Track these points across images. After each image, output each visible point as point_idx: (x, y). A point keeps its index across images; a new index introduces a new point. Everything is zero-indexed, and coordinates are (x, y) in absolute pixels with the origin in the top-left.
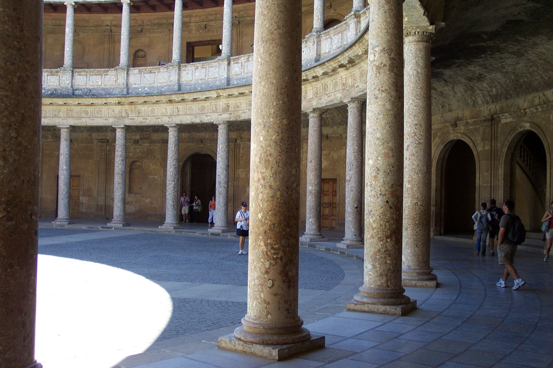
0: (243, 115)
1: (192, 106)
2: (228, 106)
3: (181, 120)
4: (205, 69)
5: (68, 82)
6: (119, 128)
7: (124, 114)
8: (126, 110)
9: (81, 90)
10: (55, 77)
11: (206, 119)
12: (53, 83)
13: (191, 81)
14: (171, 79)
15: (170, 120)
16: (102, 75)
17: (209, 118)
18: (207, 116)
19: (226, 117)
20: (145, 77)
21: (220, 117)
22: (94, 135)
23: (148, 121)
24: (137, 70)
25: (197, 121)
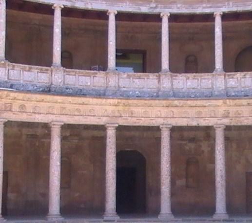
0: (246, 121)
1: (188, 110)
2: (229, 113)
3: (176, 123)
4: (197, 80)
5: (60, 81)
6: (113, 127)
7: (117, 114)
8: (118, 111)
9: (72, 89)
10: (45, 74)
11: (203, 123)
12: (44, 80)
13: (182, 89)
14: (165, 86)
15: (165, 122)
16: (90, 76)
17: (207, 121)
18: (205, 120)
19: (226, 121)
20: (134, 82)
21: (219, 122)
22: (25, 131)
23: (141, 122)
24: (126, 75)
25: (194, 123)
